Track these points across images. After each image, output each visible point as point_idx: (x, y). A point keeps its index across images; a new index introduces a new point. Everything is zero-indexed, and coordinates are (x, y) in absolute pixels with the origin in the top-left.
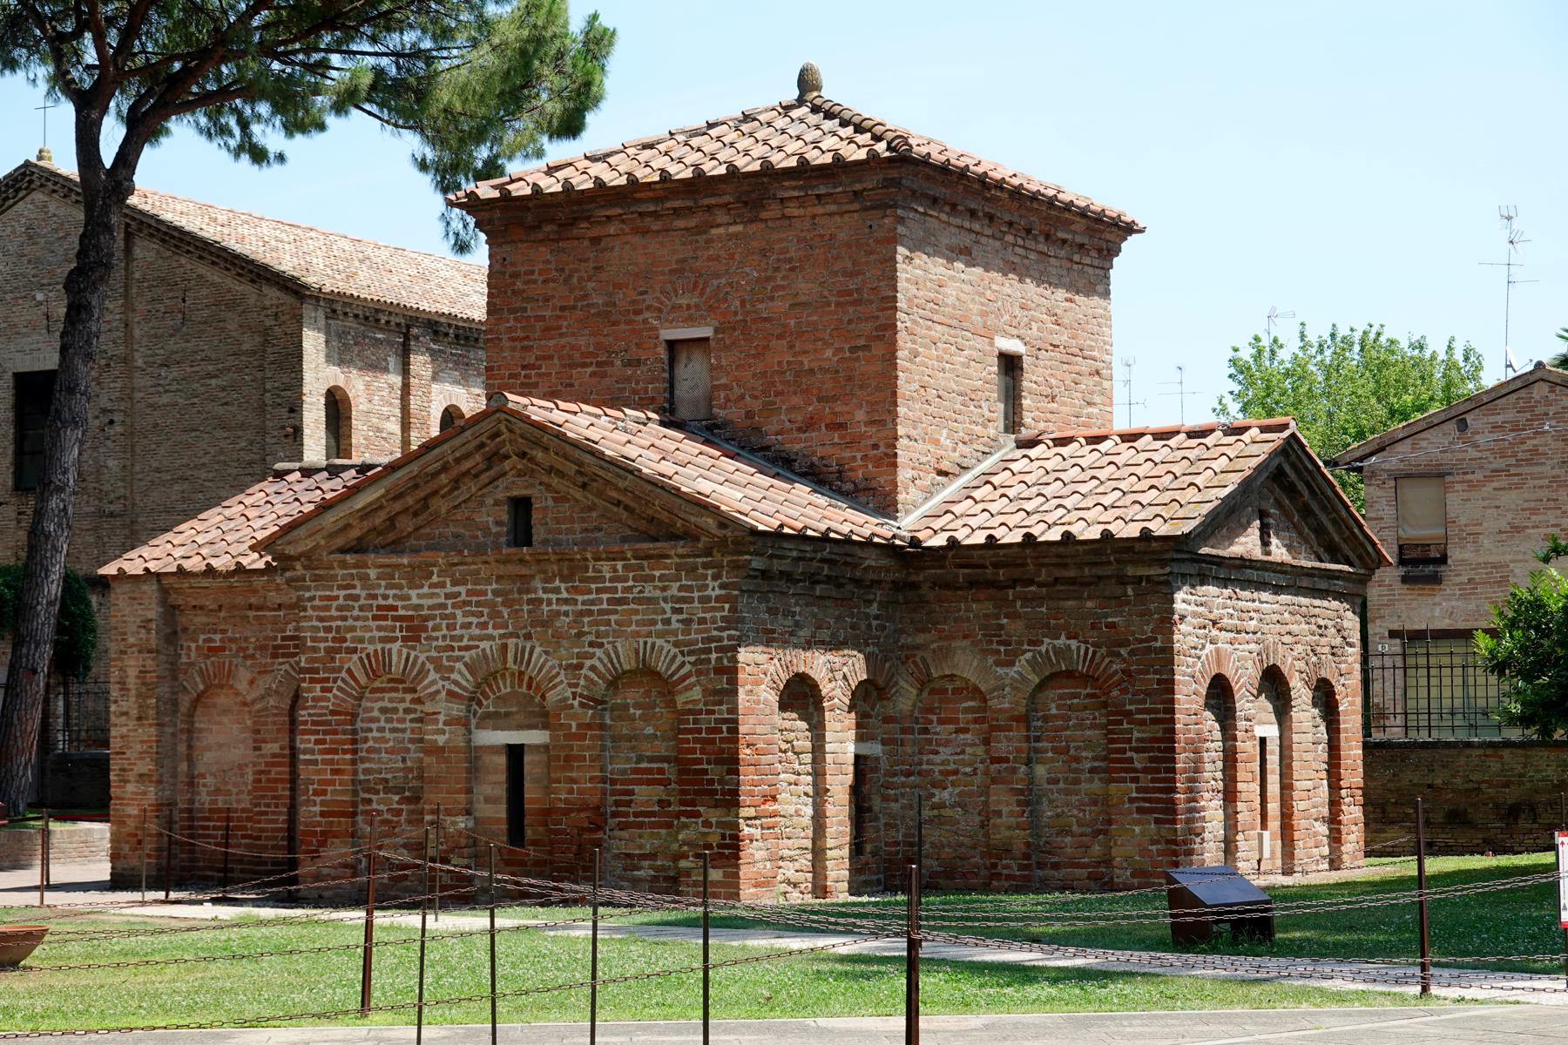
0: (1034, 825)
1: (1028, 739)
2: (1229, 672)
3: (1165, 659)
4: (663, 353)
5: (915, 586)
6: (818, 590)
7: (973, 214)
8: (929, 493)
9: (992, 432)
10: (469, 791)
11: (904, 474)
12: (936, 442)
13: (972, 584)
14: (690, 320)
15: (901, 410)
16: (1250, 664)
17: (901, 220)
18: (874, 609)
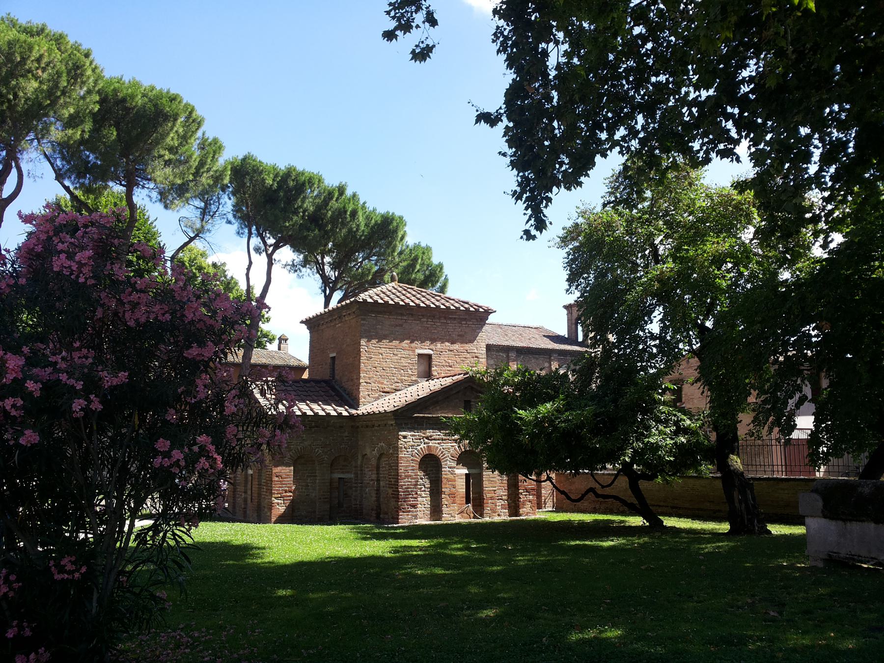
0: (378, 500)
1: (378, 474)
2: (438, 453)
3: (396, 449)
4: (329, 361)
5: (358, 427)
6: (313, 430)
7: (402, 315)
8: (377, 399)
9: (414, 378)
10: (246, 486)
11: (361, 394)
12: (382, 383)
13: (367, 426)
14: (333, 352)
15: (362, 375)
16: (452, 451)
17: (364, 320)
18: (346, 434)
